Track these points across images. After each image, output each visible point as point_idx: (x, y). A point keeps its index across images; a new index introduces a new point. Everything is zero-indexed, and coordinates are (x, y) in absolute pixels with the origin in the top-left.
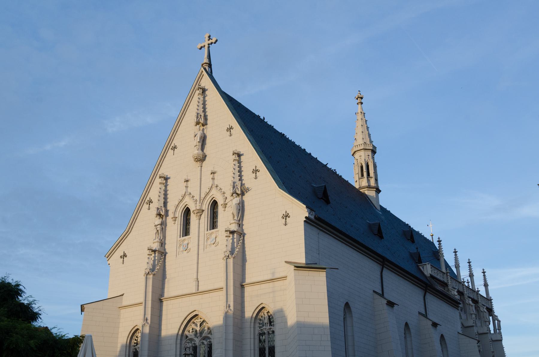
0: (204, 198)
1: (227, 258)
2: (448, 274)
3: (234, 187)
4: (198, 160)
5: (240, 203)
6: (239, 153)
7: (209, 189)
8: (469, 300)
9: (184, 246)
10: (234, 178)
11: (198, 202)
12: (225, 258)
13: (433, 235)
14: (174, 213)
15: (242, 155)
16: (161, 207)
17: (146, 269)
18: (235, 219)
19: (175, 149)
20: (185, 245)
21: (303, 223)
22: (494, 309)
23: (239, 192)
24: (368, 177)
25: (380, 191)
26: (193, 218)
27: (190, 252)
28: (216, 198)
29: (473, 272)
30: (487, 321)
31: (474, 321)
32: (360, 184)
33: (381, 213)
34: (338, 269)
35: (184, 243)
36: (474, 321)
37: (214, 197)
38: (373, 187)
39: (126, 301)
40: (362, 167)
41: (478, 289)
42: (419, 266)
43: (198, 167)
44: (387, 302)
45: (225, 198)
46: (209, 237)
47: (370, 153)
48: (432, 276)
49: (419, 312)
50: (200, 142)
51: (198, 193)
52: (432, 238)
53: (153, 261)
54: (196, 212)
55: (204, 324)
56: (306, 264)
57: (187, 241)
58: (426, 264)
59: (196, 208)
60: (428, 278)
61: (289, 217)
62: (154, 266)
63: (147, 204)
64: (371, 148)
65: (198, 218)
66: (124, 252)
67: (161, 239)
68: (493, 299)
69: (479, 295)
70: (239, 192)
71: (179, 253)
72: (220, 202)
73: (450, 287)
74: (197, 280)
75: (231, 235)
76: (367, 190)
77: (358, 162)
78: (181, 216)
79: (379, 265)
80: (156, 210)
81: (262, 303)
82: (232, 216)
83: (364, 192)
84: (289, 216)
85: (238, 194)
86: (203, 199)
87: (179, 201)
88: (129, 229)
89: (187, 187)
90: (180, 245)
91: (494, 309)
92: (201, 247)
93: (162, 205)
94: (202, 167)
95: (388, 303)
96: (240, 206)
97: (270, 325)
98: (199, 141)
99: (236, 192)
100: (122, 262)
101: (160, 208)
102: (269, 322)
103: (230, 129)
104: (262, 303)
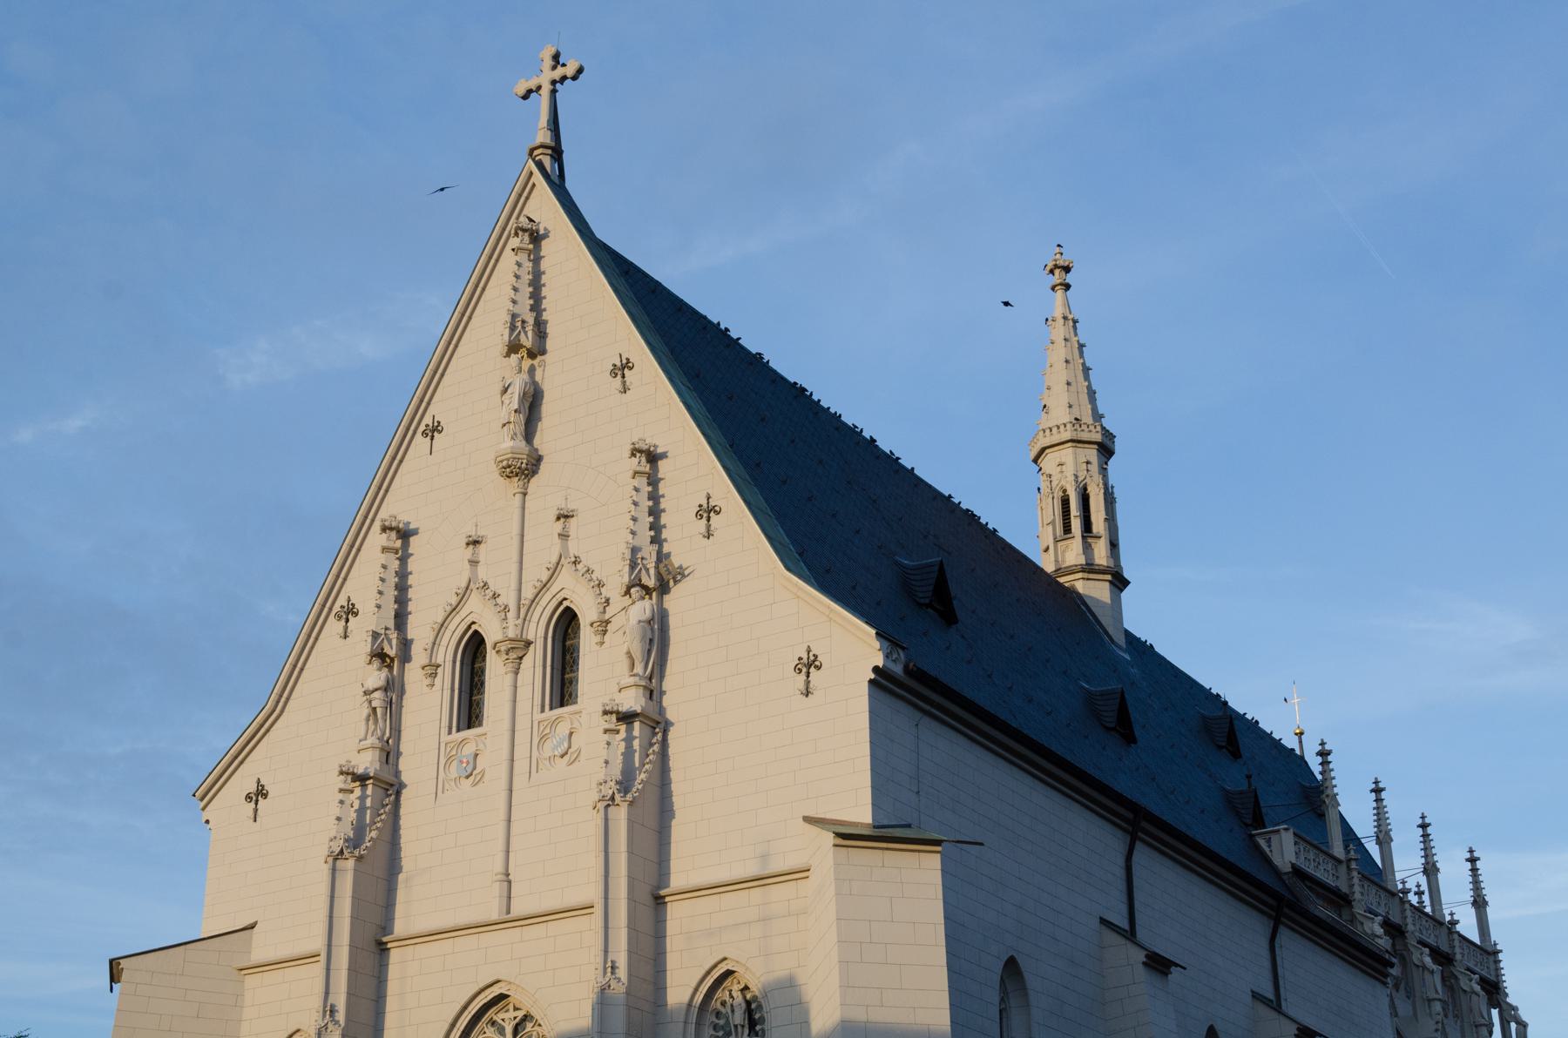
0: (533, 601)
1: (609, 805)
2: (1353, 865)
3: (633, 565)
4: (512, 472)
5: (653, 619)
6: (652, 449)
7: (549, 569)
8: (1422, 954)
9: (461, 762)
10: (633, 533)
11: (511, 615)
12: (601, 805)
13: (1302, 733)
14: (429, 651)
15: (664, 456)
16: (386, 629)
17: (331, 840)
18: (635, 671)
19: (436, 434)
20: (465, 760)
21: (864, 688)
22: (1505, 984)
23: (651, 582)
24: (1085, 535)
25: (1126, 583)
26: (495, 668)
27: (481, 784)
28: (571, 602)
29: (1435, 858)
30: (1481, 1025)
31: (1437, 1023)
32: (1060, 559)
33: (1127, 657)
34: (981, 844)
35: (464, 753)
36: (1437, 1023)
37: (565, 599)
38: (1101, 568)
39: (262, 947)
40: (1065, 502)
41: (1452, 914)
42: (1254, 836)
43: (514, 495)
44: (1146, 956)
45: (603, 600)
46: (547, 731)
47: (1092, 454)
48: (1297, 871)
49: (1252, 992)
50: (520, 413)
51: (514, 585)
52: (1301, 742)
53: (356, 811)
54: (503, 649)
55: (529, 1026)
56: (874, 827)
57: (474, 744)
58: (1278, 831)
59: (504, 633)
60: (1285, 877)
61: (818, 668)
62: (360, 829)
63: (340, 618)
64: (1098, 437)
65: (510, 667)
66: (259, 781)
67: (385, 739)
68: (1501, 951)
69: (1456, 936)
70: (651, 582)
71: (447, 786)
72: (587, 615)
73: (1359, 909)
74: (504, 877)
75: (623, 728)
76: (1083, 579)
77: (1054, 484)
78: (454, 662)
79: (1119, 833)
80: (370, 639)
81: (725, 959)
82: (626, 663)
83: (1073, 586)
84: (817, 663)
85: (645, 588)
86: (527, 602)
87: (449, 609)
88: (278, 702)
89: (474, 563)
90: (449, 759)
91: (1505, 984)
92: (521, 765)
93: (391, 624)
94: (525, 494)
95: (1148, 962)
96: (652, 630)
98: (516, 407)
99: (640, 580)
100: (251, 814)
101: (383, 632)
102: (746, 1022)
104: (725, 959)
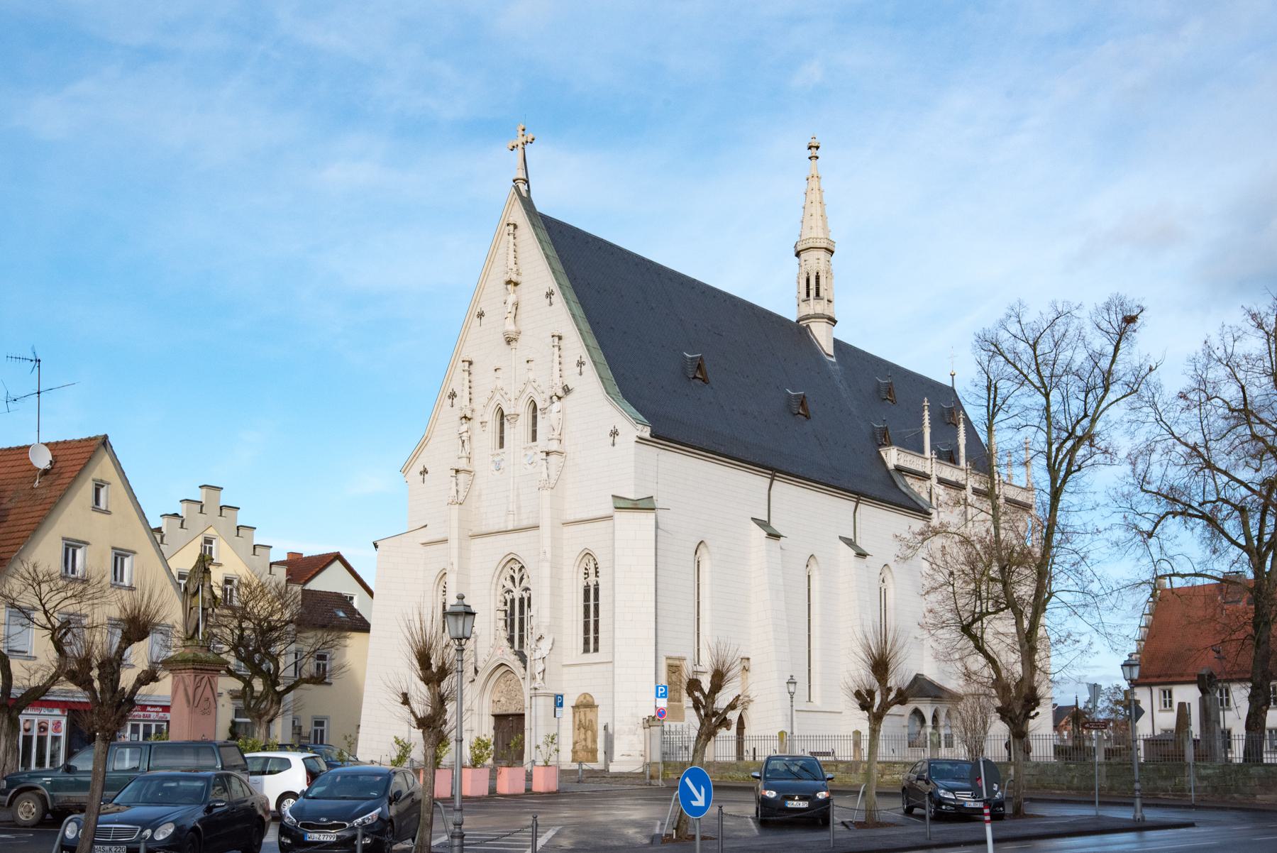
2: (934, 460)
33: (834, 360)
48: (899, 469)
70: (560, 393)
83: (808, 326)
97: (597, 576)
103: (550, 295)
